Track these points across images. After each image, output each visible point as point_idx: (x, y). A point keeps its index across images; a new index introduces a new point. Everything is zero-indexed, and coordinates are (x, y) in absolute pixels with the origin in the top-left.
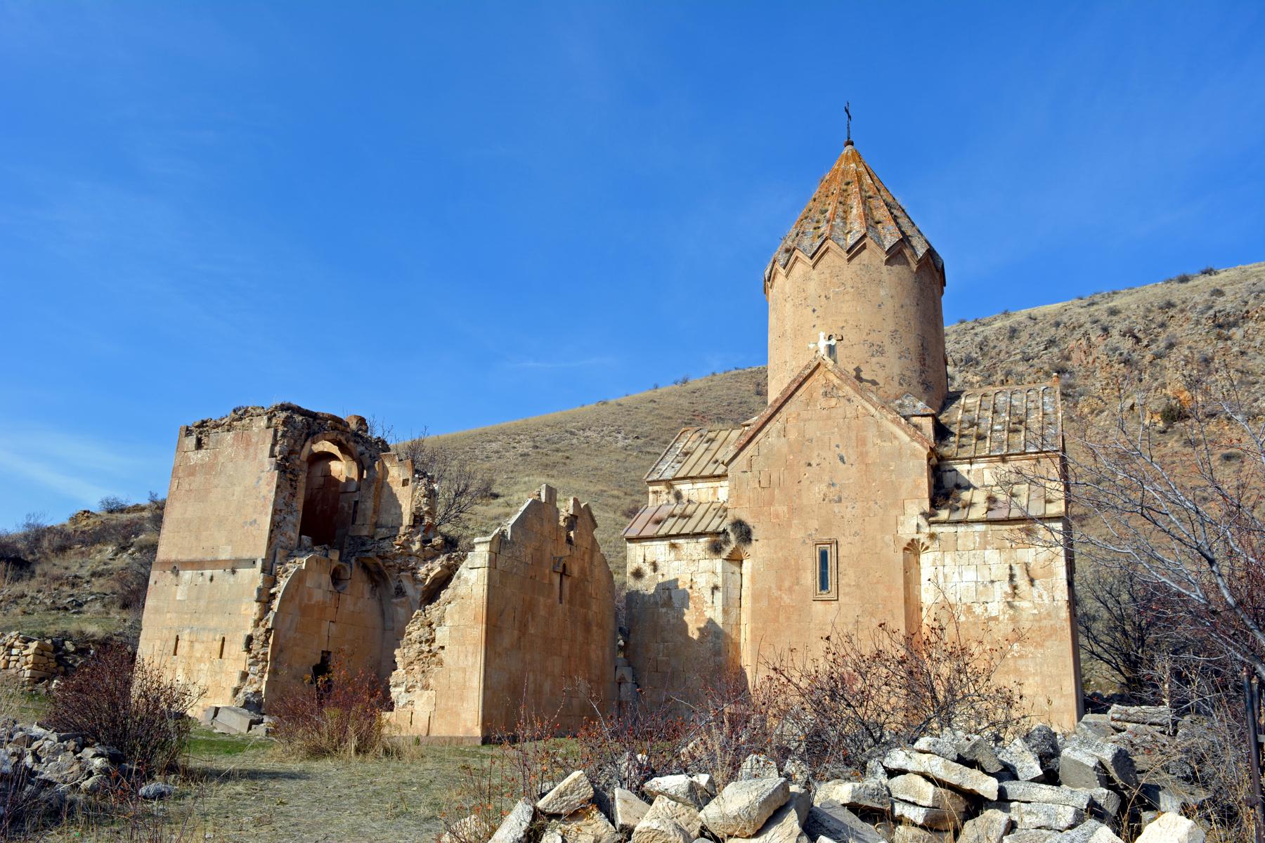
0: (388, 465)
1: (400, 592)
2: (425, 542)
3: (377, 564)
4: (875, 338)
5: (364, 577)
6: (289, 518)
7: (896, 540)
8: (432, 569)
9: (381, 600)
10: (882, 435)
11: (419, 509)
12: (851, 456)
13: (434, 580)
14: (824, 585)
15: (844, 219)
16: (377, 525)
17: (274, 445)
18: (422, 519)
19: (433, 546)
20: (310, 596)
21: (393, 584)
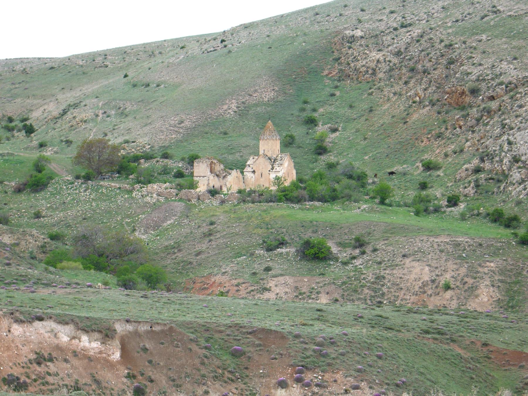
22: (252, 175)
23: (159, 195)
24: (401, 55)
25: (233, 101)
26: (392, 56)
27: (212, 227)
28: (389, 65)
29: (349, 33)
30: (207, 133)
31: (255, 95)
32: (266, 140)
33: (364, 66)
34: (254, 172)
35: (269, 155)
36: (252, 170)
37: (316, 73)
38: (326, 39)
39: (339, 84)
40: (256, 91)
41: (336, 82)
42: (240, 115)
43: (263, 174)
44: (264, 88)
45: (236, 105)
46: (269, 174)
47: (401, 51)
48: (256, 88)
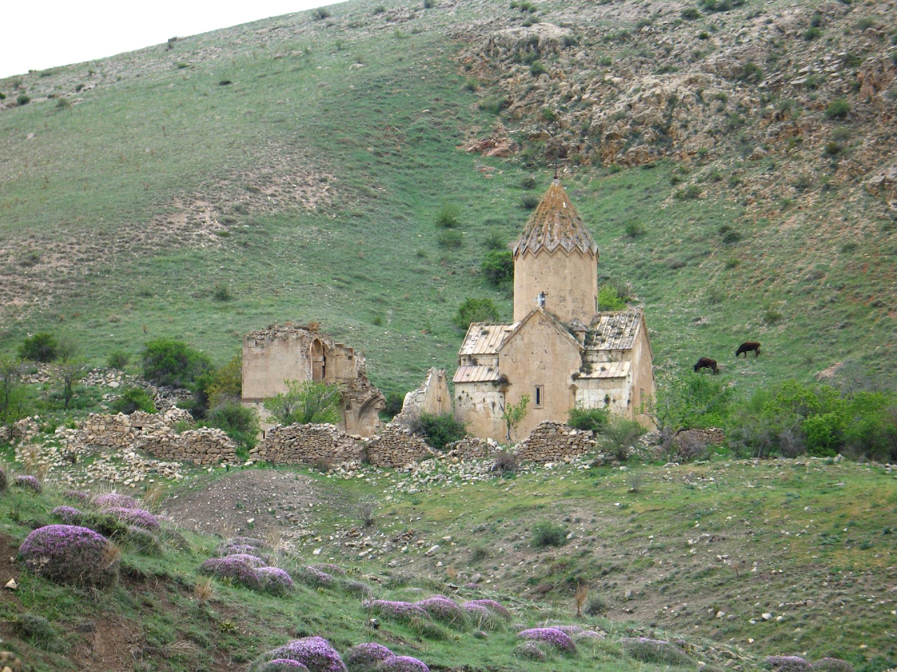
1: (349, 408)
4: (562, 293)
7: (566, 384)
10: (561, 342)
12: (550, 350)
14: (538, 402)
15: (551, 232)
22: (493, 395)
23: (151, 455)
24: (759, 79)
25: (199, 203)
26: (724, 83)
27: (557, 554)
28: (720, 110)
29: (517, 33)
30: (147, 295)
31: (269, 192)
32: (552, 253)
33: (619, 117)
34: (502, 383)
35: (565, 312)
36: (494, 377)
37: (436, 145)
38: (431, 54)
39: (533, 177)
40: (267, 180)
41: (519, 171)
42: (245, 245)
43: (547, 389)
44: (289, 173)
45: (216, 214)
46: (574, 389)
47: (754, 69)
48: (265, 171)
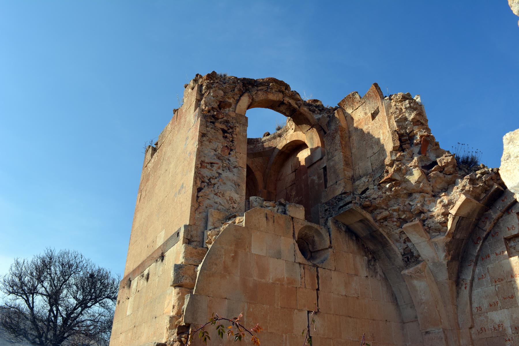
0: (349, 111)
1: (411, 257)
2: (427, 167)
3: (363, 221)
5: (353, 246)
6: (226, 174)
8: (451, 203)
9: (386, 279)
11: (401, 121)
13: (460, 219)
16: (353, 179)
17: (198, 101)
18: (411, 137)
19: (442, 169)
20: (263, 272)
21: (398, 249)
